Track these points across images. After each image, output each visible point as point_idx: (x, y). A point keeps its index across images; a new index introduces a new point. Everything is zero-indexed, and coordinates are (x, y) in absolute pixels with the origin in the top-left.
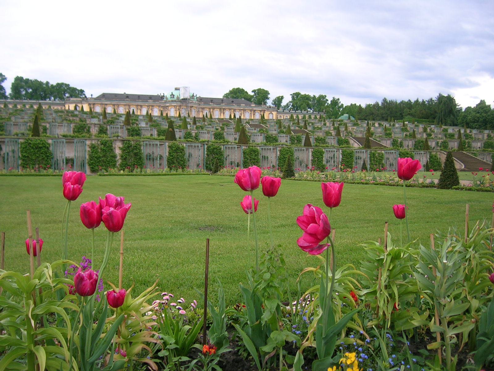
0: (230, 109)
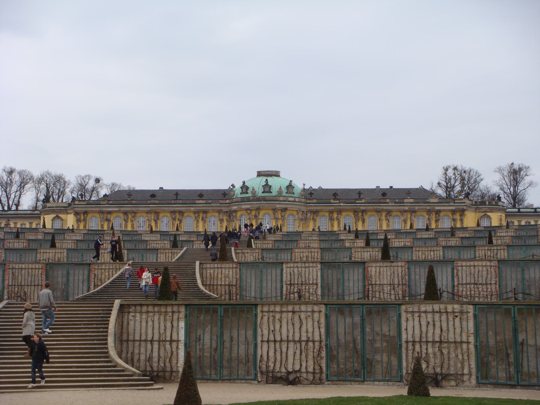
0: (378, 212)
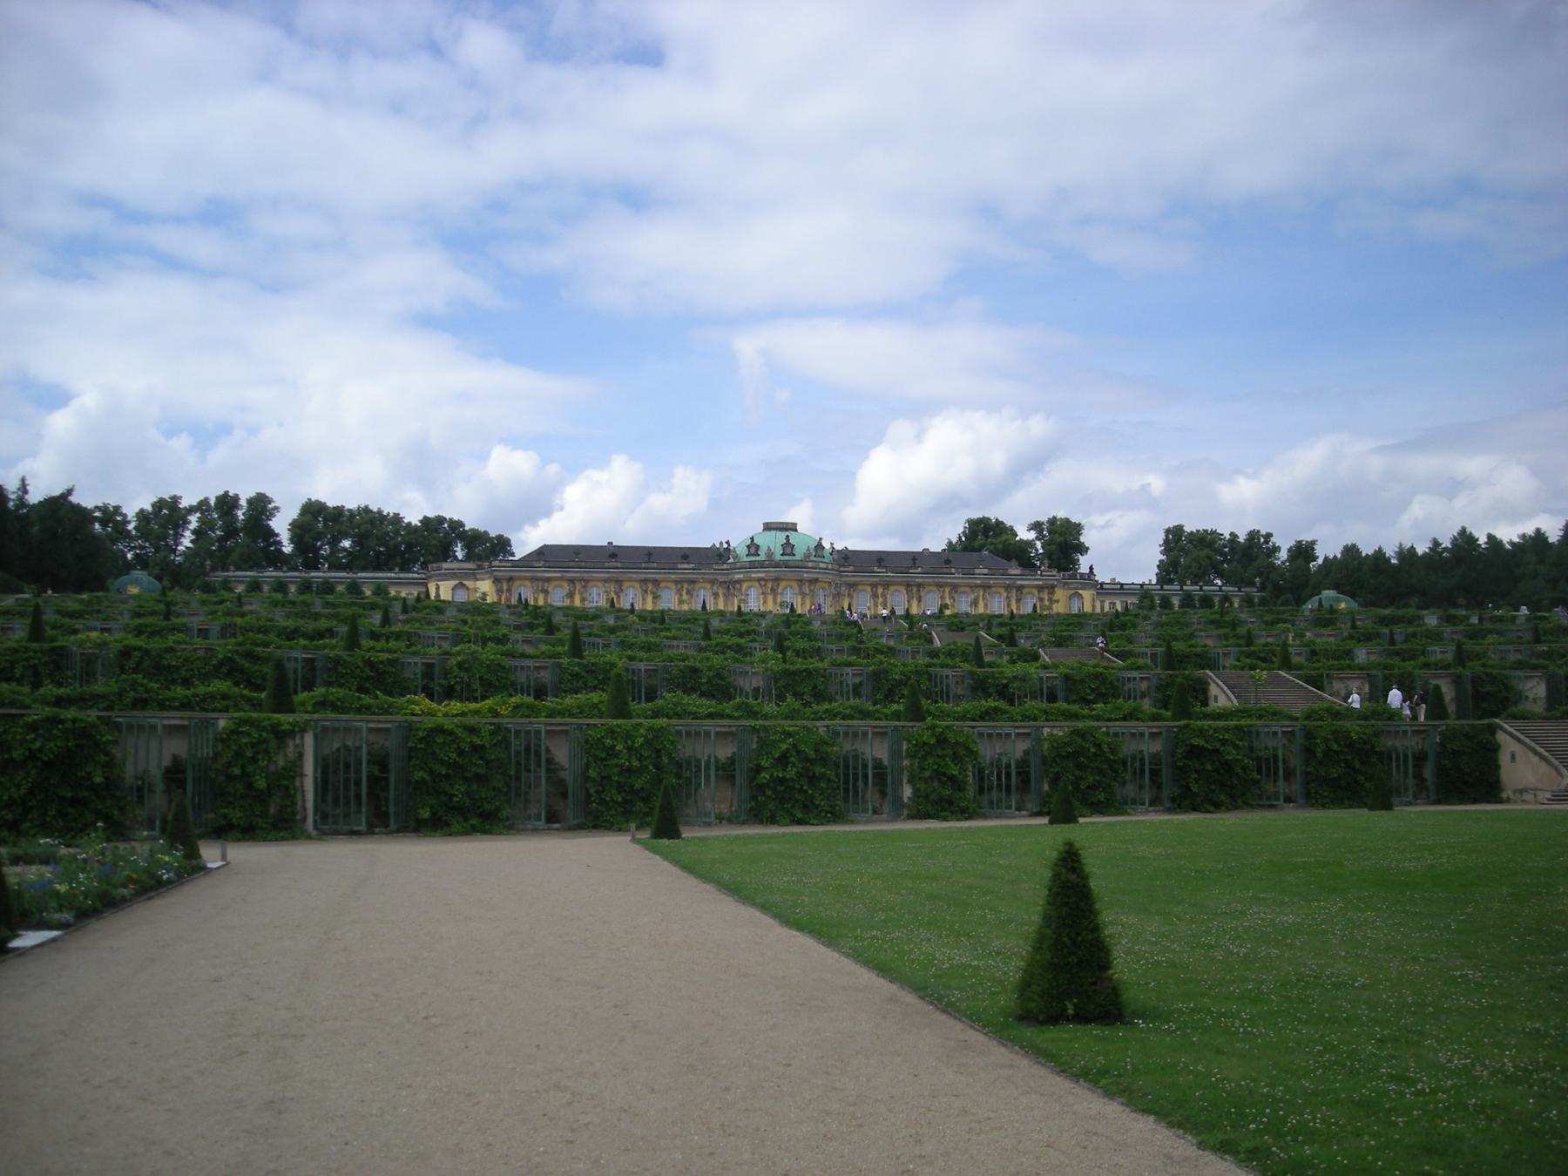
0: (940, 586)
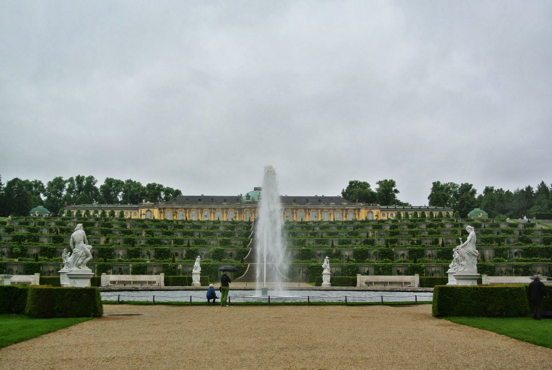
0: (317, 209)
